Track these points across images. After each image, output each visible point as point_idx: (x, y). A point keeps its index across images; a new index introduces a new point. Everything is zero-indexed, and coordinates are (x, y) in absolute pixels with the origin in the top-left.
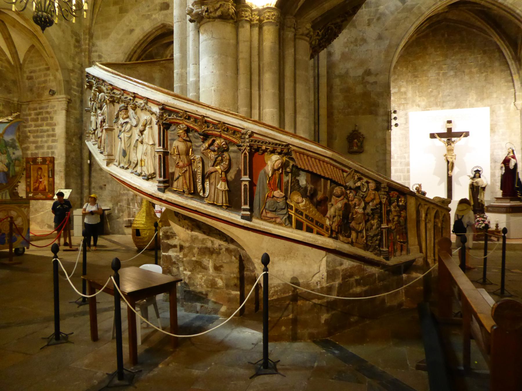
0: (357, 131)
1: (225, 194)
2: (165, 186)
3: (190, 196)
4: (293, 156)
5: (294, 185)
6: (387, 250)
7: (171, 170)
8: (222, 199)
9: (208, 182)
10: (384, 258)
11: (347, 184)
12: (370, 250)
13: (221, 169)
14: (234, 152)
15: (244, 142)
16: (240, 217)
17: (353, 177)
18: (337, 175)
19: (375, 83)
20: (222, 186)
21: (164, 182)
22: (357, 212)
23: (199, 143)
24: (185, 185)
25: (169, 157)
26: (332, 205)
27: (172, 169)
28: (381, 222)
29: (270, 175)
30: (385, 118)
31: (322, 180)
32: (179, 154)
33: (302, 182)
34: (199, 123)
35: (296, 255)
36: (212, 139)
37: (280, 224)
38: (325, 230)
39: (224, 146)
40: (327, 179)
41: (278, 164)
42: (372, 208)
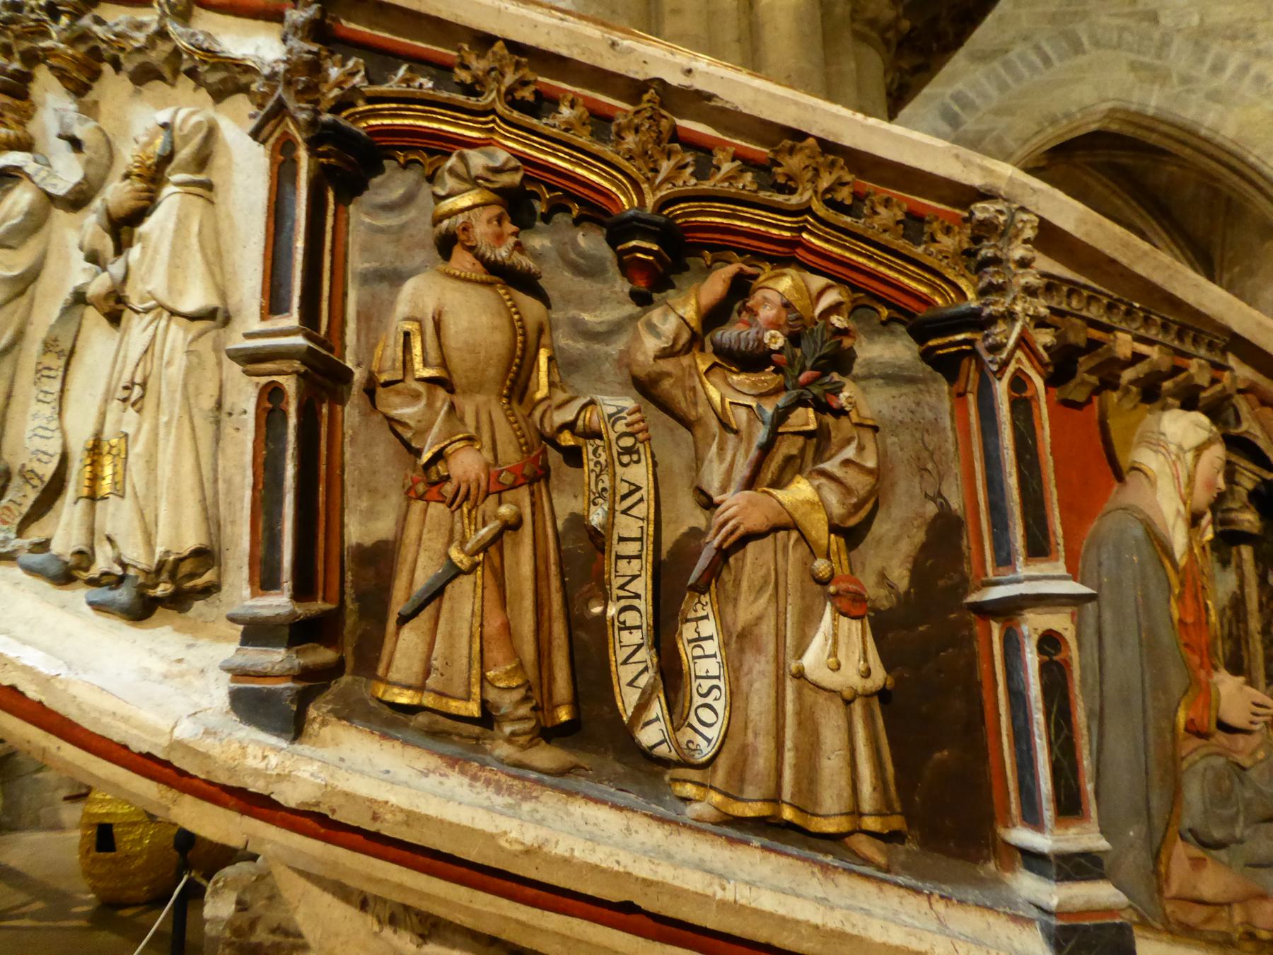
2: (304, 674)
3: (546, 756)
7: (361, 526)
8: (848, 771)
9: (708, 628)
13: (823, 503)
14: (893, 377)
15: (1000, 289)
20: (838, 654)
21: (297, 633)
23: (609, 303)
24: (496, 653)
25: (351, 414)
27: (371, 514)
32: (443, 383)
34: (630, 140)
36: (729, 270)
39: (838, 321)
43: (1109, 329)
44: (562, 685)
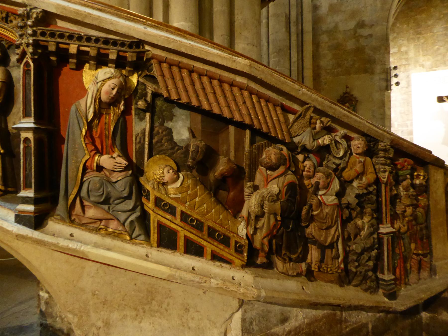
0: (348, 93)
4: (155, 72)
6: (393, 277)
10: (385, 295)
11: (296, 140)
12: (354, 283)
17: (311, 123)
18: (268, 118)
19: (371, 36)
22: (320, 204)
26: (256, 188)
28: (379, 221)
30: (383, 76)
31: (232, 129)
33: (179, 133)
35: (165, 306)
37: (115, 235)
38: (233, 251)
40: (241, 126)
41: (108, 89)
42: (357, 192)
43: (68, 44)
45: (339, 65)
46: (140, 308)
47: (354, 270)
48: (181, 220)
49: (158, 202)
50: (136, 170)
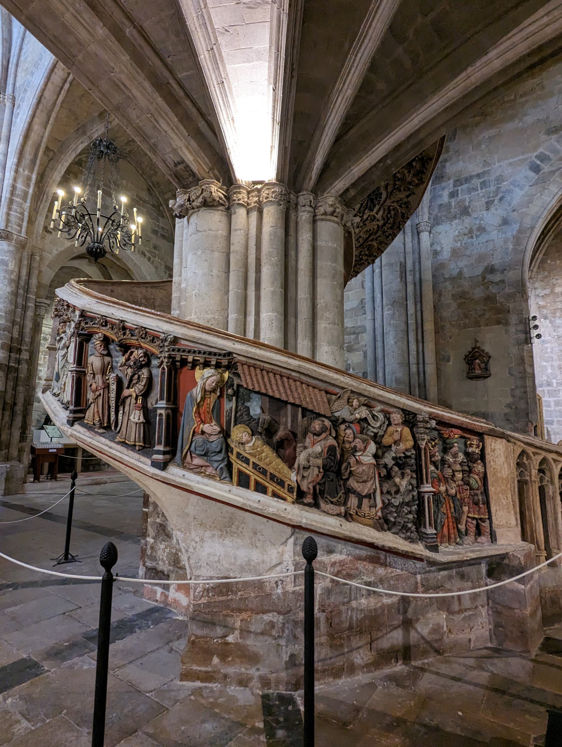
0: (479, 348)
1: (140, 427)
2: (74, 418)
4: (240, 371)
5: (241, 415)
6: (435, 532)
10: (427, 547)
11: (337, 414)
12: (393, 531)
16: (149, 462)
17: (349, 402)
18: (315, 401)
19: (503, 281)
22: (358, 462)
24: (96, 415)
26: (305, 448)
28: (420, 481)
29: (198, 401)
31: (289, 407)
33: (254, 410)
35: (240, 529)
37: (211, 477)
38: (286, 491)
41: (210, 383)
44: (106, 421)
45: (466, 316)
46: (224, 529)
47: (392, 519)
48: (253, 468)
49: (239, 455)
50: (226, 434)
